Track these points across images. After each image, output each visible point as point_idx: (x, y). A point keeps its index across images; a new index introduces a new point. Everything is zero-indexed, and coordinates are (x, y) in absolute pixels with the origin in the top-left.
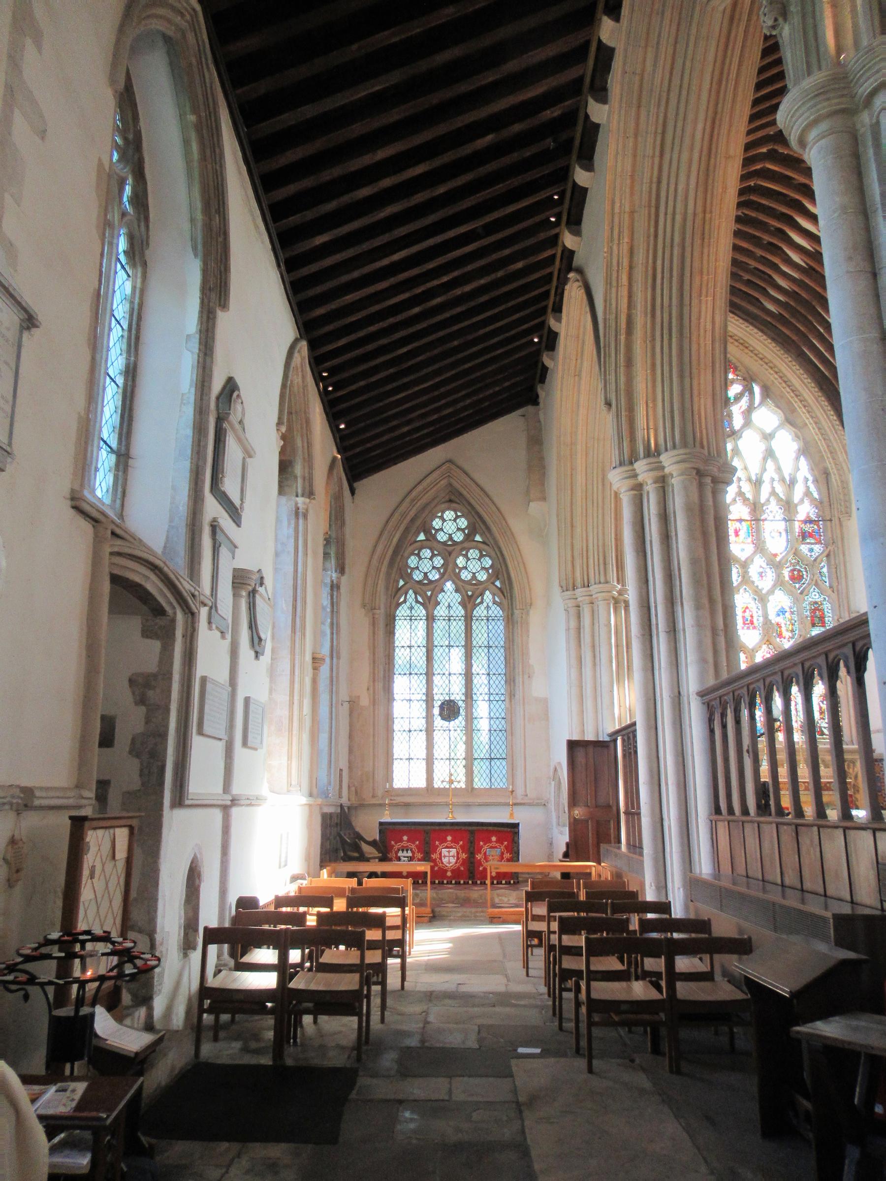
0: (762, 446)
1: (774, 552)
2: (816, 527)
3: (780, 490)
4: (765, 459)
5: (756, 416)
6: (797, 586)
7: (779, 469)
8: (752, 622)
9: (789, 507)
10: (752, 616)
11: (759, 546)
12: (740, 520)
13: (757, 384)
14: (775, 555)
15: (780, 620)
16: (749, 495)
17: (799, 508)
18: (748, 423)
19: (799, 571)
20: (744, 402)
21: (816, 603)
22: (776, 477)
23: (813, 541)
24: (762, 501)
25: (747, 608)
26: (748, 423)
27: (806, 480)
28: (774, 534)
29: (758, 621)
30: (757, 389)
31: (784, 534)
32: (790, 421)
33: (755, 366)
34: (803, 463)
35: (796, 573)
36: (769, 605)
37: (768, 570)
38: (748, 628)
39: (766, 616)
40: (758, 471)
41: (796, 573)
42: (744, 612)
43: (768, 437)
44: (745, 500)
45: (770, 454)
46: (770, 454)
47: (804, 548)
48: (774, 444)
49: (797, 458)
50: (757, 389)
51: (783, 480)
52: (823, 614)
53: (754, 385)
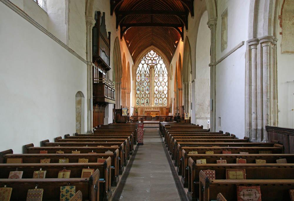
0: (160, 66)
3: (162, 72)
5: (160, 62)
7: (162, 70)
9: (163, 75)
11: (159, 80)
16: (158, 73)
18: (159, 63)
22: (162, 71)
26: (159, 63)
30: (160, 57)
32: (164, 62)
33: (160, 55)
34: (166, 68)
44: (157, 74)
51: (162, 71)
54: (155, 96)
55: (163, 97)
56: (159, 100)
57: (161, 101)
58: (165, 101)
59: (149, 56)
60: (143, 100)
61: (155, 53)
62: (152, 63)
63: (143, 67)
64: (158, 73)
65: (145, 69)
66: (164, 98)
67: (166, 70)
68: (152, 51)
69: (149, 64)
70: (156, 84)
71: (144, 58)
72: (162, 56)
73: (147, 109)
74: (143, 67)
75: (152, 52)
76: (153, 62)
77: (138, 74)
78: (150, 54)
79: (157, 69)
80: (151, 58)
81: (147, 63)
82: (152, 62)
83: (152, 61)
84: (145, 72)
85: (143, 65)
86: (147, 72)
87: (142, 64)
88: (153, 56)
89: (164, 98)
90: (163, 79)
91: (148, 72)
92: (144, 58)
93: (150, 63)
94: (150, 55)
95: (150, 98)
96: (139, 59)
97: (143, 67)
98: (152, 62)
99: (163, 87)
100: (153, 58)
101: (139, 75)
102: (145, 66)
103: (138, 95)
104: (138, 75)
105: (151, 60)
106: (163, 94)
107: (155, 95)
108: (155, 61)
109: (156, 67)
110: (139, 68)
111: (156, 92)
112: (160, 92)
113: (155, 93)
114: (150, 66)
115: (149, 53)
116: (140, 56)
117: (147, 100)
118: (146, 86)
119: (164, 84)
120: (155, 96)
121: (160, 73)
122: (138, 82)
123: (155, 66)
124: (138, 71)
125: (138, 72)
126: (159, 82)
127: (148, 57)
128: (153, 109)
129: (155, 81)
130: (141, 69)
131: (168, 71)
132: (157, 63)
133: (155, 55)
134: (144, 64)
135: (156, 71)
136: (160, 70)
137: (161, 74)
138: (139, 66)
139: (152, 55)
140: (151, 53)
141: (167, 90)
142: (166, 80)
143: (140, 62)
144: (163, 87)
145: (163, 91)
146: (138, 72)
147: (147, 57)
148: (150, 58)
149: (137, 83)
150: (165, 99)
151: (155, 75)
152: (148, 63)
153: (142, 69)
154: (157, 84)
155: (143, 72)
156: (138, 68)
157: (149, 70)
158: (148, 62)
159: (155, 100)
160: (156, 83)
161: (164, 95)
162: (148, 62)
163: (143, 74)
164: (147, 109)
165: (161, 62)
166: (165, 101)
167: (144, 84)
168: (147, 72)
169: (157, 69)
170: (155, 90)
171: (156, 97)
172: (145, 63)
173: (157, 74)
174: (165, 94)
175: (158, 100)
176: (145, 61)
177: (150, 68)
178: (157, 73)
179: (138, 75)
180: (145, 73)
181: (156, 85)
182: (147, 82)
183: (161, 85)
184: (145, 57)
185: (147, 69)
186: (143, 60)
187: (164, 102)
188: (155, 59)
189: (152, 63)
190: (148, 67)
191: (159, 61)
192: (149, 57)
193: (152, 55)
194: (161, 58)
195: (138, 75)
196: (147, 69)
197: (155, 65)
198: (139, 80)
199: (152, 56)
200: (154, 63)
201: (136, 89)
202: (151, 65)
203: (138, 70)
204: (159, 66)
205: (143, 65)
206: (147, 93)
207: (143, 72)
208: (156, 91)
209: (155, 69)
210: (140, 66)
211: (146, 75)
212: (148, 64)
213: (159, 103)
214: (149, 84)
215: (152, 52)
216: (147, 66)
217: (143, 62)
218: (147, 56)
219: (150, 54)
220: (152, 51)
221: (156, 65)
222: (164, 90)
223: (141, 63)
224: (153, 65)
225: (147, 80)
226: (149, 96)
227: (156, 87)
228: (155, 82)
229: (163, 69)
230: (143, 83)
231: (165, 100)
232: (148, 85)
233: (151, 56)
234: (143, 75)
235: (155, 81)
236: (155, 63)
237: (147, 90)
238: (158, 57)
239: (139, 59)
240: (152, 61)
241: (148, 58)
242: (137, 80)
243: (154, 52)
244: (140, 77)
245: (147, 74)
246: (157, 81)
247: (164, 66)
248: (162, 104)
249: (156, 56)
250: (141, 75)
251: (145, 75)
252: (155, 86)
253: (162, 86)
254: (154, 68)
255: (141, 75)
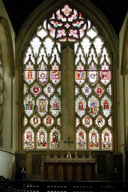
1: (92, 82)
2: (108, 73)
3: (95, 60)
4: (90, 49)
6: (99, 94)
7: (95, 52)
8: (82, 108)
9: (99, 67)
10: (82, 105)
11: (87, 81)
12: (80, 71)
13: (89, 21)
14: (92, 83)
15: (92, 107)
16: (84, 62)
17: (102, 67)
18: (85, 35)
19: (101, 89)
20: (85, 28)
21: (106, 100)
22: (94, 55)
23: (106, 78)
24: (88, 64)
25: (81, 102)
27: (105, 56)
28: (92, 76)
29: (85, 107)
30: (89, 23)
31: (96, 76)
32: (100, 34)
34: (105, 50)
35: (99, 90)
36: (89, 102)
37: (89, 89)
38: (81, 110)
39: (87, 106)
40: (88, 53)
41: (99, 90)
42: (80, 104)
43: (92, 40)
45: (92, 46)
46: (92, 46)
47: (103, 81)
48: (94, 43)
49: (102, 49)
50: (89, 23)
51: (96, 56)
52: (108, 104)
53: (88, 21)
54: (78, 123)
55: (101, 125)
56: (90, 135)
57: (94, 138)
58: (107, 137)
59: (59, 18)
60: (42, 133)
61: (75, 12)
62: (67, 36)
63: (42, 45)
64: (84, 62)
65: (49, 51)
66: (103, 128)
67: (107, 55)
68: (67, 7)
69: (59, 38)
70: (80, 91)
71: (45, 23)
72: (94, 17)
73: (52, 156)
74: (42, 45)
75: (67, 9)
76: (70, 35)
77: (30, 63)
78: (62, 13)
79: (80, 51)
80: (64, 23)
81: (53, 35)
82: (67, 34)
83: (67, 31)
84: (49, 59)
85: (42, 40)
86: (53, 59)
87: (38, 40)
88: (70, 20)
89: (103, 128)
90: (100, 78)
91: (55, 60)
92: (45, 23)
93: (63, 37)
94: (60, 17)
95: (64, 128)
96: (30, 22)
97: (42, 45)
98: (67, 34)
99: (100, 99)
100: (70, 23)
101: (32, 67)
102: (49, 43)
103: (29, 119)
104: (27, 67)
105: (65, 28)
106: (100, 116)
107: (78, 120)
108: (76, 31)
109: (80, 46)
110: (32, 48)
111: (81, 113)
112: (92, 112)
113: (76, 115)
114: (62, 43)
115: (58, 12)
116: (36, 12)
117: (54, 134)
118: (52, 96)
119: (103, 91)
120: (78, 123)
121: (89, 62)
122: (29, 86)
123: (76, 45)
124: (30, 55)
125: (30, 60)
126: (87, 86)
127: (56, 20)
128: (73, 156)
129: (78, 81)
130: (36, 51)
131: (111, 55)
132: (82, 35)
133: (74, 17)
134: (45, 38)
135: (78, 55)
136: (90, 52)
137: (93, 64)
138: (32, 43)
139: (67, 15)
140: (63, 10)
141: (110, 104)
142: (106, 81)
143: (34, 34)
144: (100, 99)
145: (100, 107)
146: (30, 60)
147: (52, 22)
148: (60, 25)
149: (25, 90)
150: (106, 130)
151: (75, 67)
152: (56, 36)
153: (39, 52)
154: (84, 90)
155: (43, 60)
156: (29, 50)
157: (61, 55)
158: (56, 33)
159: (77, 134)
160: (80, 88)
161: (104, 120)
162: (56, 33)
163: (43, 64)
164: (52, 156)
165: (92, 33)
166: (107, 137)
167: (46, 90)
168: (53, 59)
169: (80, 51)
170: (77, 107)
171: (81, 125)
172: (49, 36)
173: (80, 64)
174: (107, 116)
175: (85, 134)
176: (48, 31)
177: (62, 48)
178: (80, 61)
179: (30, 67)
180: (49, 62)
181: (81, 93)
182: (53, 85)
183: (93, 93)
184: (48, 22)
185: (52, 52)
186: (43, 28)
187: (103, 140)
188: (75, 25)
189: (67, 36)
190: (55, 46)
191: (85, 31)
192: (60, 21)
193: (67, 15)
194: (92, 25)
195: (30, 67)
196: (52, 52)
197: (74, 40)
198: (32, 81)
199: (67, 18)
200: (72, 37)
201: (22, 103)
202: (65, 40)
203: (27, 54)
204: (86, 43)
205: (42, 40)
206: (53, 113)
207: (43, 60)
208: (81, 108)
209: (77, 52)
210: (35, 43)
211: (51, 68)
212: (55, 40)
213: (90, 140)
214: (59, 90)
215: (67, 9)
216: (53, 44)
217: (42, 33)
218: (53, 18)
219: (62, 13)
220: (67, 7)
221: (80, 40)
222: (102, 104)
223: (37, 36)
224: (70, 40)
225: (53, 81)
226: (59, 124)
227: (80, 99)
228: (78, 85)
229: (98, 51)
230: (43, 87)
231: (107, 134)
232: (56, 93)
233: (64, 20)
234: (43, 67)
235: (75, 84)
236: (76, 36)
237: (56, 105)
238: (82, 22)
239: (30, 22)
240: (67, 31)
241: (56, 25)
242: (27, 81)
243: (71, 10)
244: (34, 72)
245: (55, 64)
246: (83, 81)
247: (99, 43)
248: (97, 146)
249: (80, 20)
250: (36, 67)
251: (49, 68)
252: (77, 96)
253: (97, 96)
254: (73, 48)
255: (36, 67)
